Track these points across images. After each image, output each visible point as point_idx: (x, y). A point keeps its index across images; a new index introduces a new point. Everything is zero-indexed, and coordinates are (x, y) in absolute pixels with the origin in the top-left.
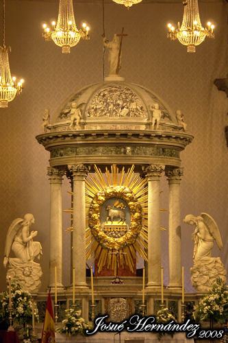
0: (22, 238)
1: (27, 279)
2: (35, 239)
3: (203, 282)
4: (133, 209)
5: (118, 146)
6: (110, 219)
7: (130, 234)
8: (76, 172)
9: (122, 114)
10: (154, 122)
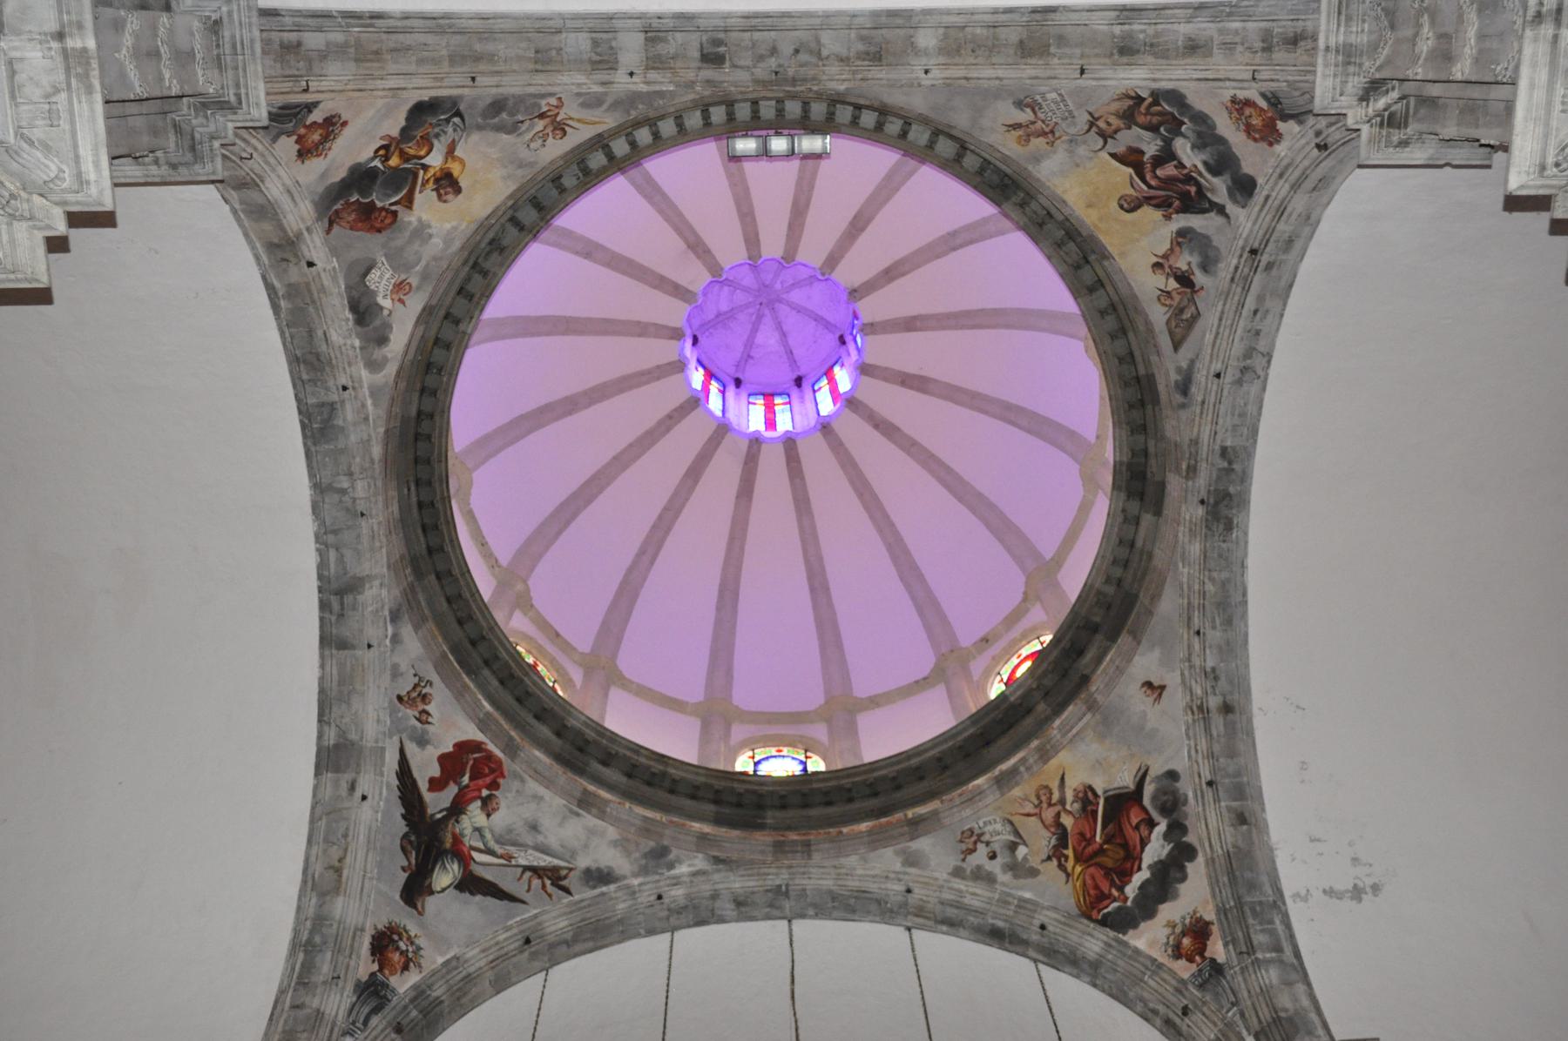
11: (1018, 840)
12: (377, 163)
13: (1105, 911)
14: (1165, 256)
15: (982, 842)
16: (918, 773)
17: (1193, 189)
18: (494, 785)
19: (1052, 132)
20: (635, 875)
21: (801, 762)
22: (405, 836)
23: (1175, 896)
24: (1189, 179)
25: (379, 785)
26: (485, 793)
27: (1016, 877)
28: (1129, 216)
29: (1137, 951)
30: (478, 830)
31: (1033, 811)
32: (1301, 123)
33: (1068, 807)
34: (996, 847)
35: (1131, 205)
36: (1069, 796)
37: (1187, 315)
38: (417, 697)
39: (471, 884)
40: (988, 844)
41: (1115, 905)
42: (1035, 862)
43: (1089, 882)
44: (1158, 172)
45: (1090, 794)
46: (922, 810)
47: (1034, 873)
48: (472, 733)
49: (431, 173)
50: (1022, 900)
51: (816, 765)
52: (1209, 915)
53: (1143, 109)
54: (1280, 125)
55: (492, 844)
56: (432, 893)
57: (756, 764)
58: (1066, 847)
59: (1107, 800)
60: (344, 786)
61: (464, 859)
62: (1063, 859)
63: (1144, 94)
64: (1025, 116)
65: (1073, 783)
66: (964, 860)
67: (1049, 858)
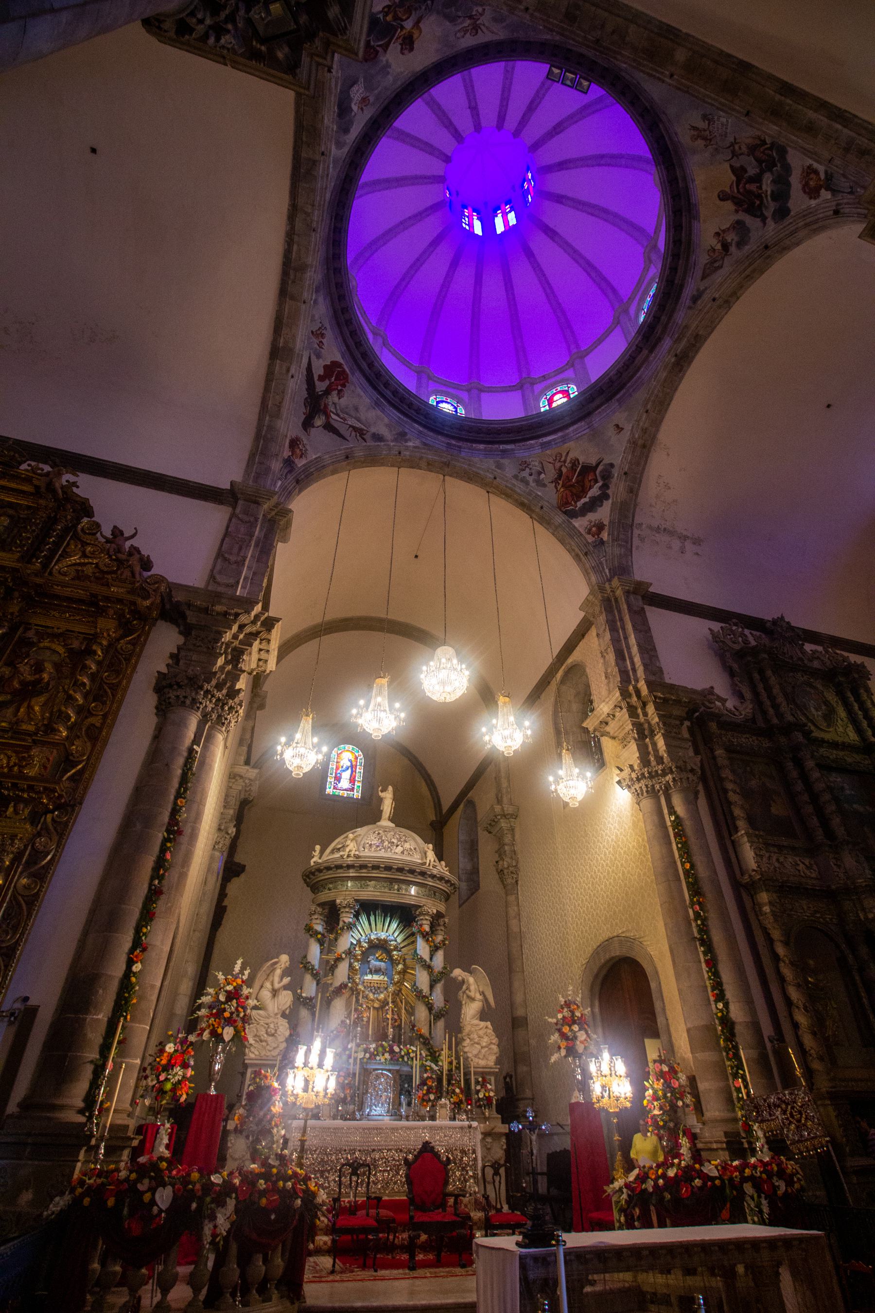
0: (272, 985)
1: (270, 1039)
2: (285, 988)
3: (475, 1052)
4: (397, 959)
5: (392, 881)
6: (371, 973)
7: (391, 989)
8: (345, 907)
9: (397, 851)
10: (428, 862)
12: (381, 16)
14: (724, 231)
16: (509, 431)
17: (758, 202)
18: (344, 386)
19: (710, 140)
20: (392, 441)
21: (455, 408)
22: (306, 399)
23: (596, 511)
24: (759, 197)
25: (298, 372)
26: (340, 388)
28: (718, 202)
29: (574, 526)
30: (334, 404)
32: (833, 195)
34: (533, 471)
35: (723, 197)
36: (568, 461)
37: (716, 265)
38: (319, 334)
39: (329, 427)
42: (546, 482)
44: (747, 186)
46: (509, 447)
47: (544, 485)
48: (338, 358)
49: (404, 31)
51: (461, 411)
52: (606, 522)
53: (762, 149)
54: (823, 191)
55: (339, 412)
56: (313, 427)
57: (438, 403)
60: (284, 368)
61: (328, 416)
63: (768, 141)
64: (702, 125)
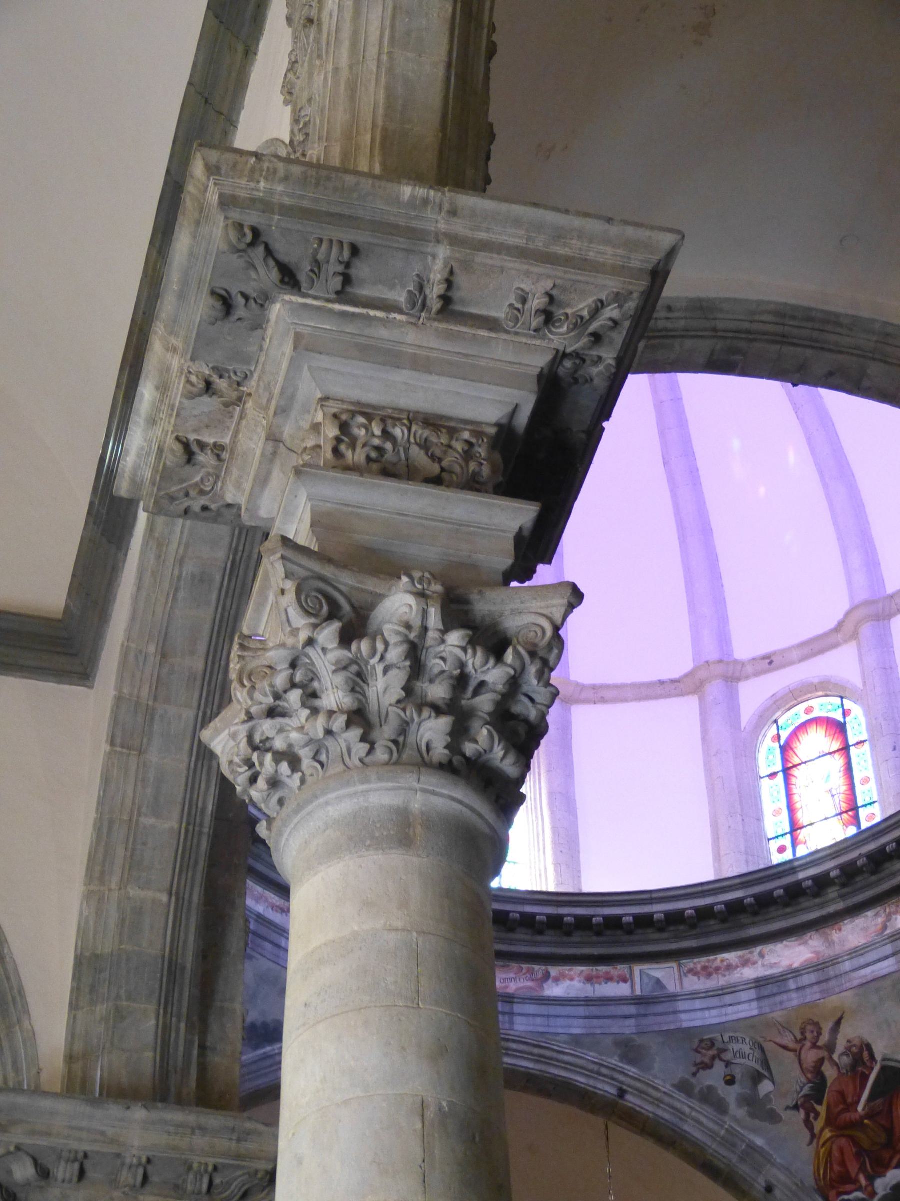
11: (766, 1074)
13: (846, 1197)
15: (721, 1060)
27: (752, 1115)
31: (791, 1045)
33: (836, 1057)
34: (738, 1072)
40: (728, 1064)
41: (859, 1195)
42: (778, 1105)
43: (836, 1154)
45: (866, 1054)
47: (773, 1117)
50: (752, 1147)
58: (820, 1103)
59: (883, 1069)
62: (812, 1115)
65: (849, 1032)
66: (694, 1075)
67: (796, 1107)
